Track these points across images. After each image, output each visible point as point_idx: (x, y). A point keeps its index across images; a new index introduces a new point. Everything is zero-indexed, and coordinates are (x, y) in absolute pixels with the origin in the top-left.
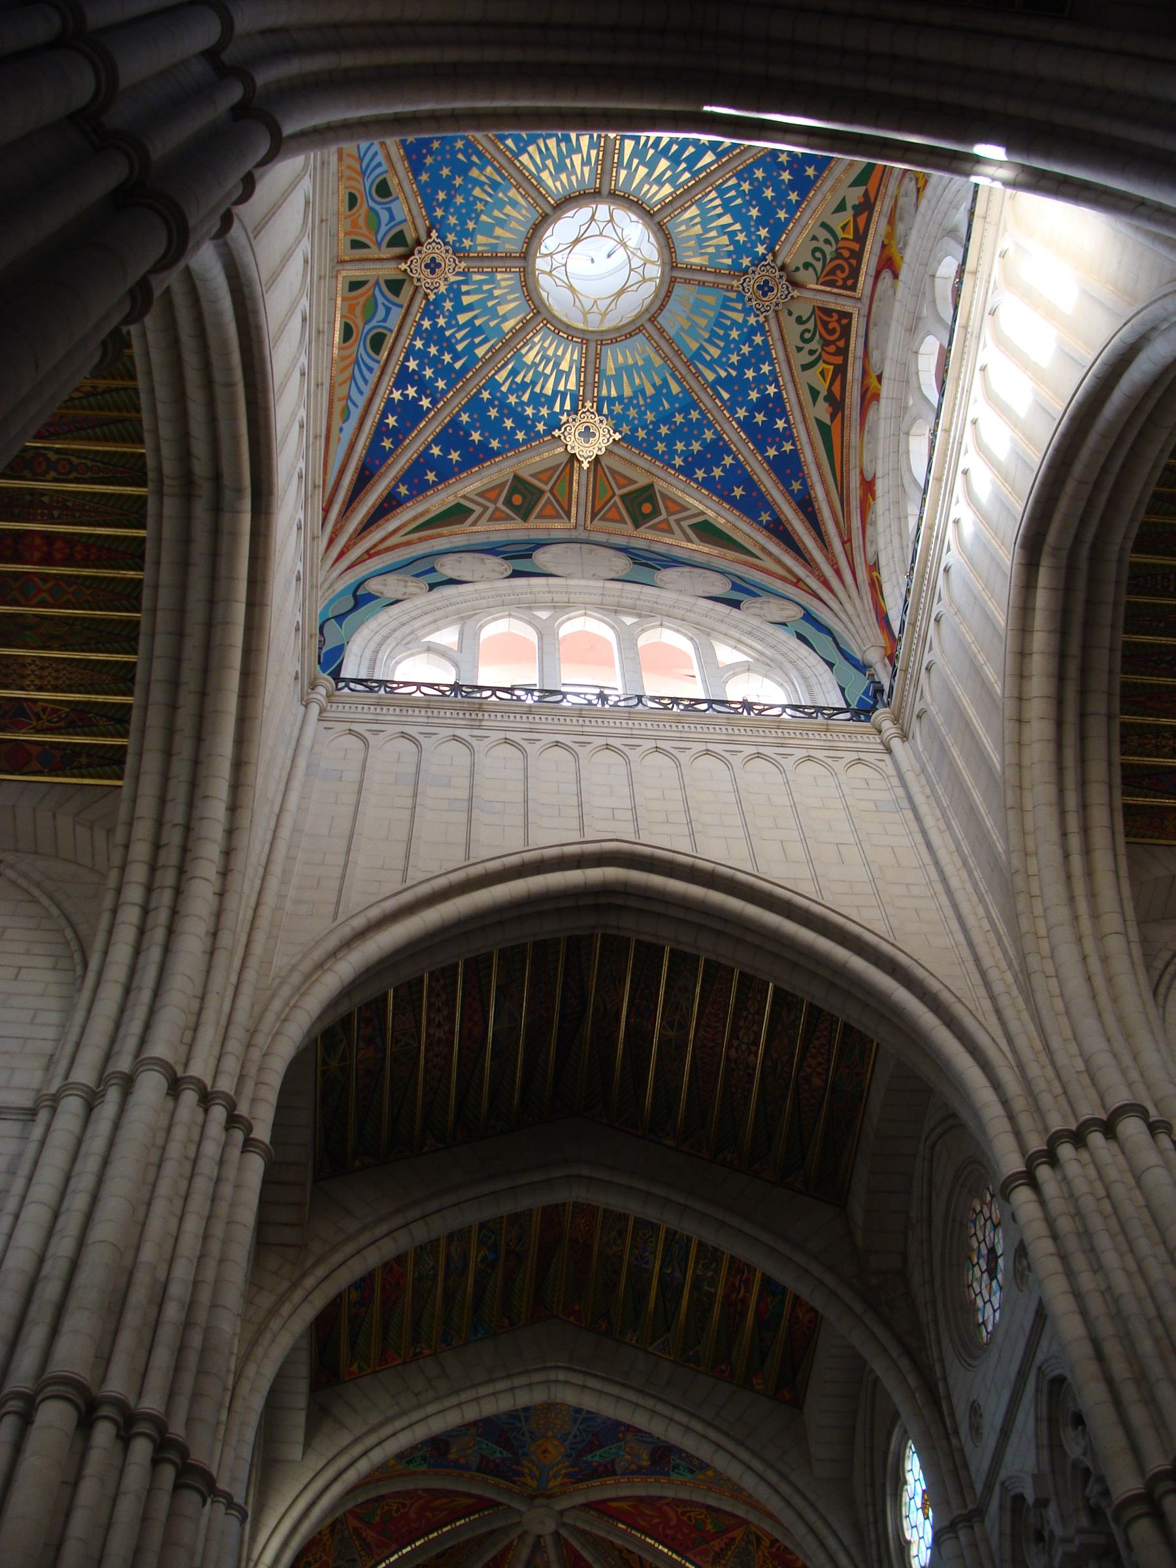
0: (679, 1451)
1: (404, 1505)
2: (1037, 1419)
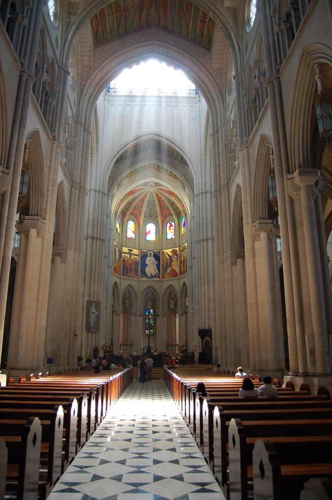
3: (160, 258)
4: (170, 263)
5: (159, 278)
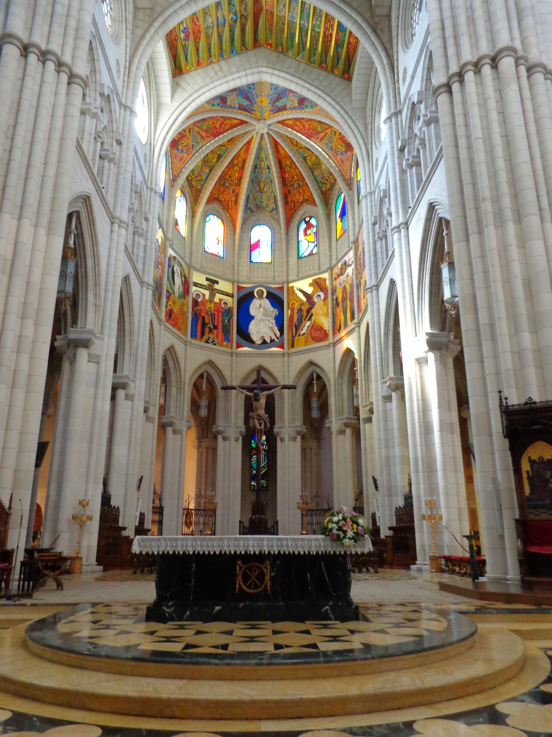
0: (308, 99)
1: (214, 123)
2: (424, 68)
3: (283, 302)
4: (309, 311)
5: (282, 346)
